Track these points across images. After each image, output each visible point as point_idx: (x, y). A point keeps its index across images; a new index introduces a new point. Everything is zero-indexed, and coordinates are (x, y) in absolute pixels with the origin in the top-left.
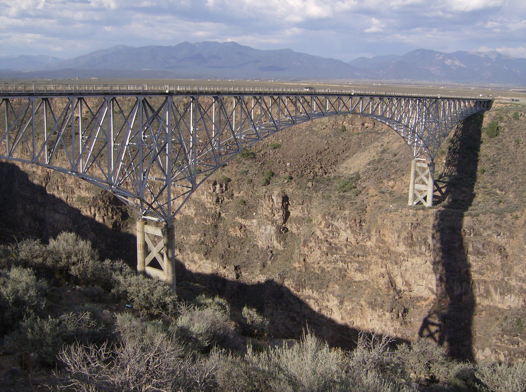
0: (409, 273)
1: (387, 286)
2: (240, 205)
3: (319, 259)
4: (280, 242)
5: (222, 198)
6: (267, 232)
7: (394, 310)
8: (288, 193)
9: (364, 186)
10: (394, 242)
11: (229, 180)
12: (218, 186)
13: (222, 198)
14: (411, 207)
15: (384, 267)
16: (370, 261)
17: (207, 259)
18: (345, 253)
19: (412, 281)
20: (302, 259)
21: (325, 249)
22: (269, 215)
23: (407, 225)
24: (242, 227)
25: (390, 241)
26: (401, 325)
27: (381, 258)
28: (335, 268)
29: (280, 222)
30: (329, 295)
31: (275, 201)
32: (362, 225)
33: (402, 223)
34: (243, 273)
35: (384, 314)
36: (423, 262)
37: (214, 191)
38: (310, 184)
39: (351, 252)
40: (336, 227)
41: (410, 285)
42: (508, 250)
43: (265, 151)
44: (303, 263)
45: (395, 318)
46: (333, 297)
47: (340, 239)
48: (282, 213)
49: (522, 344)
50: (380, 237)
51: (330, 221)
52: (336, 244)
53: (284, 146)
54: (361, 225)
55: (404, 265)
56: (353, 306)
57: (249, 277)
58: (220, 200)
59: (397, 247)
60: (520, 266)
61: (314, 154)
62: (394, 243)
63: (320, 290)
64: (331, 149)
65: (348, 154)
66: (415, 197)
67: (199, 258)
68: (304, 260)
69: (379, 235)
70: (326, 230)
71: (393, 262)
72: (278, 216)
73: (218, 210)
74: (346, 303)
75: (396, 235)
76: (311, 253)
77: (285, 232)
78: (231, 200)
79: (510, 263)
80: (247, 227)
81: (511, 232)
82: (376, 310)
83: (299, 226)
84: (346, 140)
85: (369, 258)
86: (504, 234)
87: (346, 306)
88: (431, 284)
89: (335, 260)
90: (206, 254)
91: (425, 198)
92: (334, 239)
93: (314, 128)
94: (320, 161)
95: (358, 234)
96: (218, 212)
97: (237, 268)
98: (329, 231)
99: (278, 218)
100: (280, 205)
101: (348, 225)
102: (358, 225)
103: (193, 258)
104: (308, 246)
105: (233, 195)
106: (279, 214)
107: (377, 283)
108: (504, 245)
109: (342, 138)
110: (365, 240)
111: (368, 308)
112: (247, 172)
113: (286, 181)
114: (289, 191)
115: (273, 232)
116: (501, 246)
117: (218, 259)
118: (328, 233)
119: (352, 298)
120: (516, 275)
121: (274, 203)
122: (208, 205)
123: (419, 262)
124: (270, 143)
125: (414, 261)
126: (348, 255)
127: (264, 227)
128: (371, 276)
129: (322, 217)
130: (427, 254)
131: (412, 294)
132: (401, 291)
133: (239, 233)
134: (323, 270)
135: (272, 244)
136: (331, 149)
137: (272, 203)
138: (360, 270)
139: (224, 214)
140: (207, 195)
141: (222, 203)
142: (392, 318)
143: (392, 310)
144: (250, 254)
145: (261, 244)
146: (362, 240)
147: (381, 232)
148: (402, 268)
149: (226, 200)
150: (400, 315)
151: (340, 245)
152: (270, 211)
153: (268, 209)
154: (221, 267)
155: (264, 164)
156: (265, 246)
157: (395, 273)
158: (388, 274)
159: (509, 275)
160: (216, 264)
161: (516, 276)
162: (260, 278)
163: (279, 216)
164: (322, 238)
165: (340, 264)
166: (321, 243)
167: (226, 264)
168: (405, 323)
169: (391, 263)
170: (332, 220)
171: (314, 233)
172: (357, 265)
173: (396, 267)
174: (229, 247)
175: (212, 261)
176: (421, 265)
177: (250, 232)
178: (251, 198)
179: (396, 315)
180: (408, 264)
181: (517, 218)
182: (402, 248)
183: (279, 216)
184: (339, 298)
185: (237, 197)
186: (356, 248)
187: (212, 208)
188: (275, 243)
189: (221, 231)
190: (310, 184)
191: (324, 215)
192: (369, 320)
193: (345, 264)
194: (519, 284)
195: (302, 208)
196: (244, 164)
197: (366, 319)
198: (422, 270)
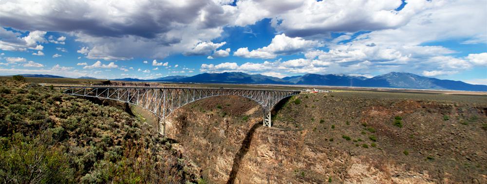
12: (209, 117)
114: (229, 119)
125: (264, 145)
134: (235, 146)
181: (302, 133)
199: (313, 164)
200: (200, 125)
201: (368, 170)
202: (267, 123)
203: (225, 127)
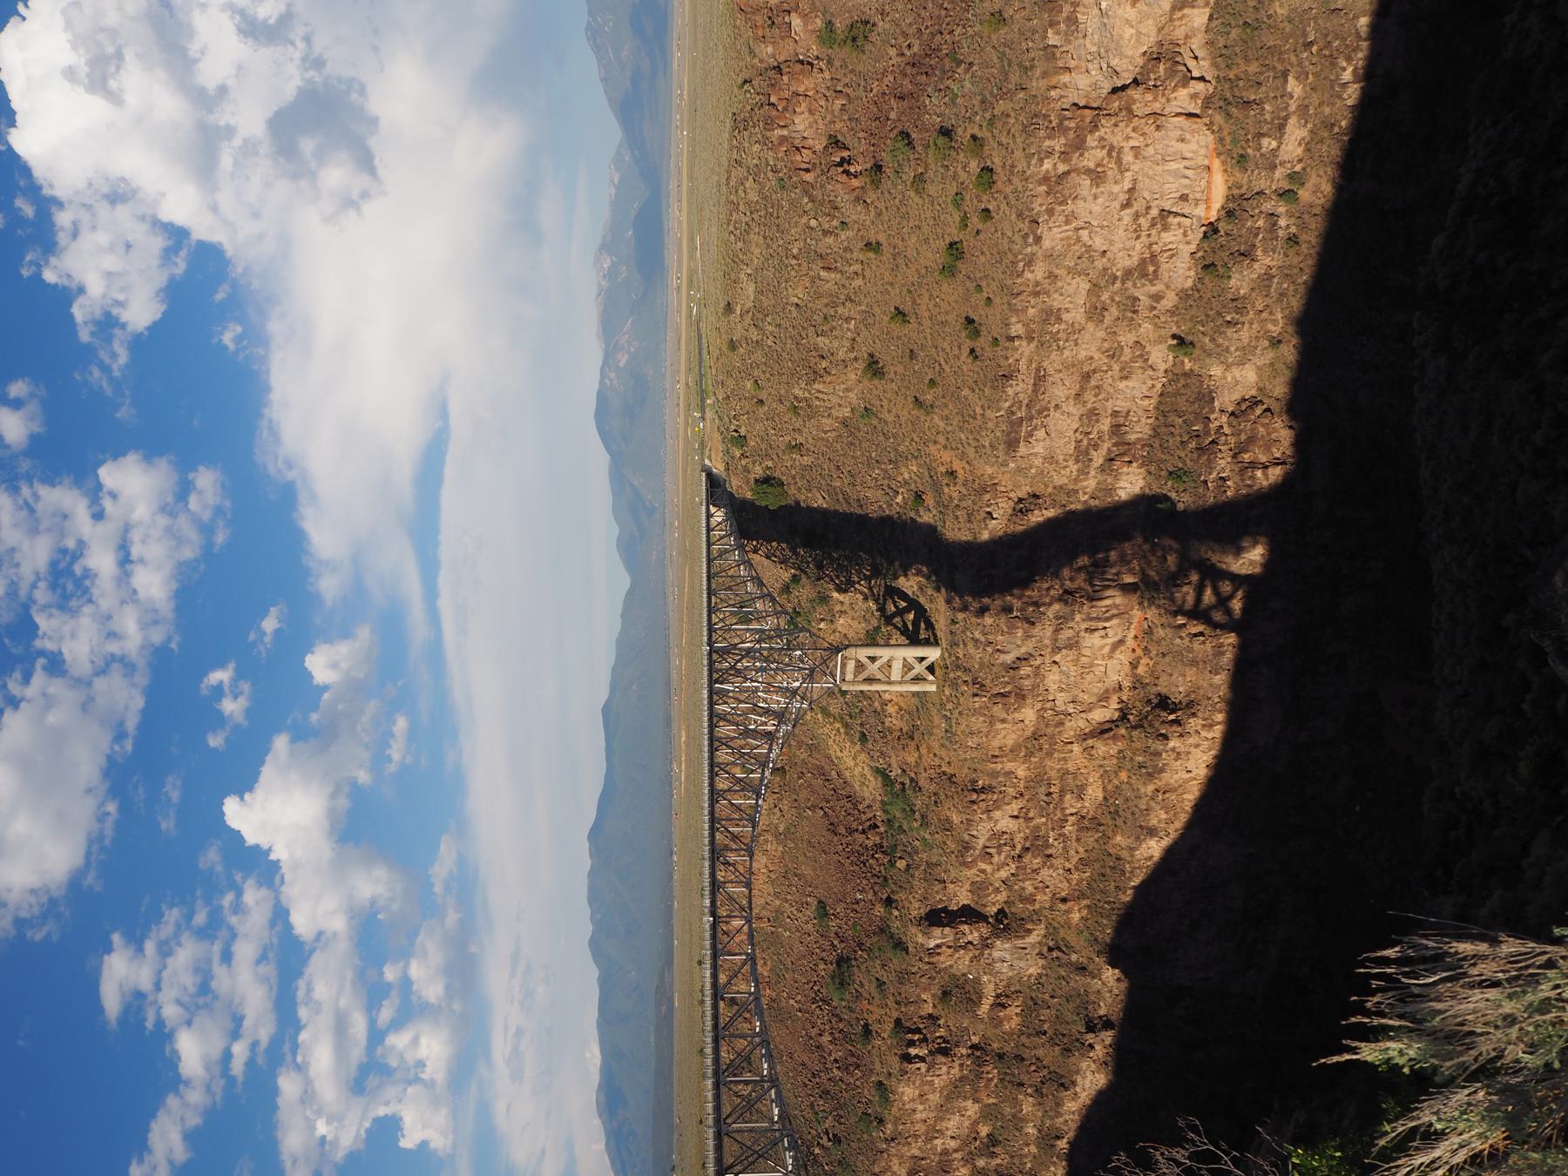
0: (1081, 695)
1: (1111, 742)
2: (952, 1003)
3: (1061, 871)
4: (1029, 931)
5: (938, 1041)
6: (1008, 957)
7: (1164, 731)
8: (921, 911)
9: (900, 771)
10: (1015, 728)
11: (898, 1022)
12: (913, 1051)
13: (938, 1041)
14: (941, 688)
15: (1069, 747)
16: (1059, 770)
17: (1074, 1083)
18: (1043, 820)
19: (1098, 688)
20: (1063, 907)
21: (1037, 861)
22: (971, 955)
23: (977, 705)
24: (999, 1004)
25: (1014, 736)
26: (1194, 715)
27: (1050, 754)
28: (1078, 840)
29: (985, 930)
30: (1139, 857)
31: (939, 941)
32: (983, 788)
33: (973, 715)
34: (1102, 1012)
35: (1173, 749)
36: (1055, 668)
37: (922, 1059)
38: (901, 864)
39: (1042, 808)
40: (988, 840)
41: (1107, 691)
42: (1022, 493)
43: (832, 935)
44: (1069, 904)
45: (1179, 729)
46: (1142, 850)
47: (1016, 828)
48: (966, 927)
49: (1223, 470)
50: (1006, 756)
51: (977, 852)
52: (1026, 839)
53: (820, 893)
54: (983, 790)
55: (1063, 708)
56: (1159, 807)
57: (1110, 1001)
58: (943, 1045)
59: (1027, 722)
60: (1055, 474)
61: (836, 839)
62: (1018, 729)
63: (1127, 875)
64: (823, 804)
65: (834, 773)
66: (918, 679)
67: (1073, 1099)
68: (1064, 900)
69: (1002, 756)
70: (996, 859)
71: (1057, 730)
72: (972, 934)
73: (964, 1051)
74: (1154, 822)
75: (999, 726)
76: (1048, 887)
77: (1007, 918)
78: (941, 1022)
79: (1050, 490)
80: (999, 991)
81: (984, 490)
82: (1164, 765)
83: (991, 888)
84: (805, 771)
85: (1053, 773)
86: (988, 506)
87: (1159, 822)
88: (1102, 648)
89: (1061, 840)
90: (1062, 1085)
91: (922, 659)
92: (1016, 841)
93: (781, 830)
94: (851, 831)
95: (1001, 796)
96: (970, 1052)
97: (1091, 1028)
98: (999, 854)
99: (976, 934)
100: (947, 930)
101: (984, 816)
102: (983, 796)
103: (1073, 1113)
104: (1032, 895)
105: (930, 1015)
106: (967, 931)
107: (1105, 758)
108: (1012, 504)
109: (800, 778)
110: (1015, 780)
111: (1160, 780)
112: (881, 984)
113: (896, 913)
114: (917, 909)
115: (1006, 946)
116: (1014, 509)
117: (1073, 1059)
118: (1003, 857)
119: (1141, 811)
120: (1075, 480)
121: (943, 944)
122: (955, 1071)
123: (1057, 677)
124: (815, 921)
125: (1053, 687)
126: (1048, 815)
127: (997, 965)
128: (1092, 769)
129: (970, 868)
130: (1038, 662)
131: (1126, 684)
132: (1121, 710)
133: (1014, 1010)
135: (1033, 945)
136: (823, 804)
137: (944, 948)
138: (1080, 793)
139: (972, 1038)
140: (933, 1076)
141: (948, 1042)
142: (1181, 735)
143: (1162, 735)
144: (1059, 992)
145: (1033, 969)
146: (1015, 787)
147: (996, 754)
148: (1071, 711)
149: (942, 1032)
150: (1172, 717)
151: (1027, 831)
152: (962, 952)
153: (957, 955)
154: (1091, 1055)
155: (860, 945)
156: (1039, 961)
157: (1082, 724)
158: (1085, 740)
159: (1076, 492)
160: (1084, 1065)
161: (1076, 480)
162: (1111, 979)
163: (971, 932)
164: (1013, 866)
165: (1068, 829)
166: (1025, 868)
167: (1083, 1044)
168: (1190, 706)
169: (1060, 732)
170: (975, 849)
171: (1003, 882)
172: (1068, 797)
173: (1068, 724)
174: (1045, 1033)
175: (1078, 1072)
176: (1062, 672)
177: (1008, 986)
178: (934, 979)
179: (1175, 728)
180: (1061, 698)
181: (952, 473)
182: (1029, 714)
183: (971, 932)
184: (1142, 837)
185: (934, 1006)
186: (1032, 799)
187: (961, 1065)
188: (1033, 938)
189: (1009, 1048)
190: (901, 864)
191: (965, 864)
192: (1187, 776)
193: (1067, 821)
194: (1093, 473)
195: (952, 882)
196: (862, 985)
197: (1186, 781)
198: (1072, 668)
199: (1116, 429)
200: (984, 1131)
201: (1097, 176)
202: (919, 669)
203: (974, 936)
